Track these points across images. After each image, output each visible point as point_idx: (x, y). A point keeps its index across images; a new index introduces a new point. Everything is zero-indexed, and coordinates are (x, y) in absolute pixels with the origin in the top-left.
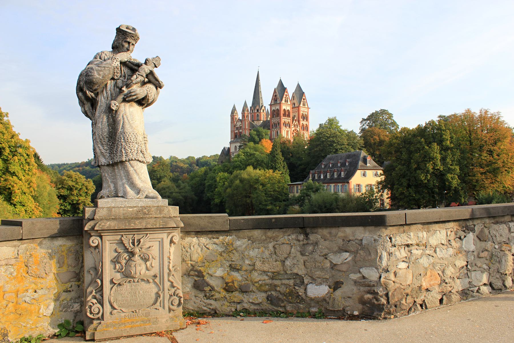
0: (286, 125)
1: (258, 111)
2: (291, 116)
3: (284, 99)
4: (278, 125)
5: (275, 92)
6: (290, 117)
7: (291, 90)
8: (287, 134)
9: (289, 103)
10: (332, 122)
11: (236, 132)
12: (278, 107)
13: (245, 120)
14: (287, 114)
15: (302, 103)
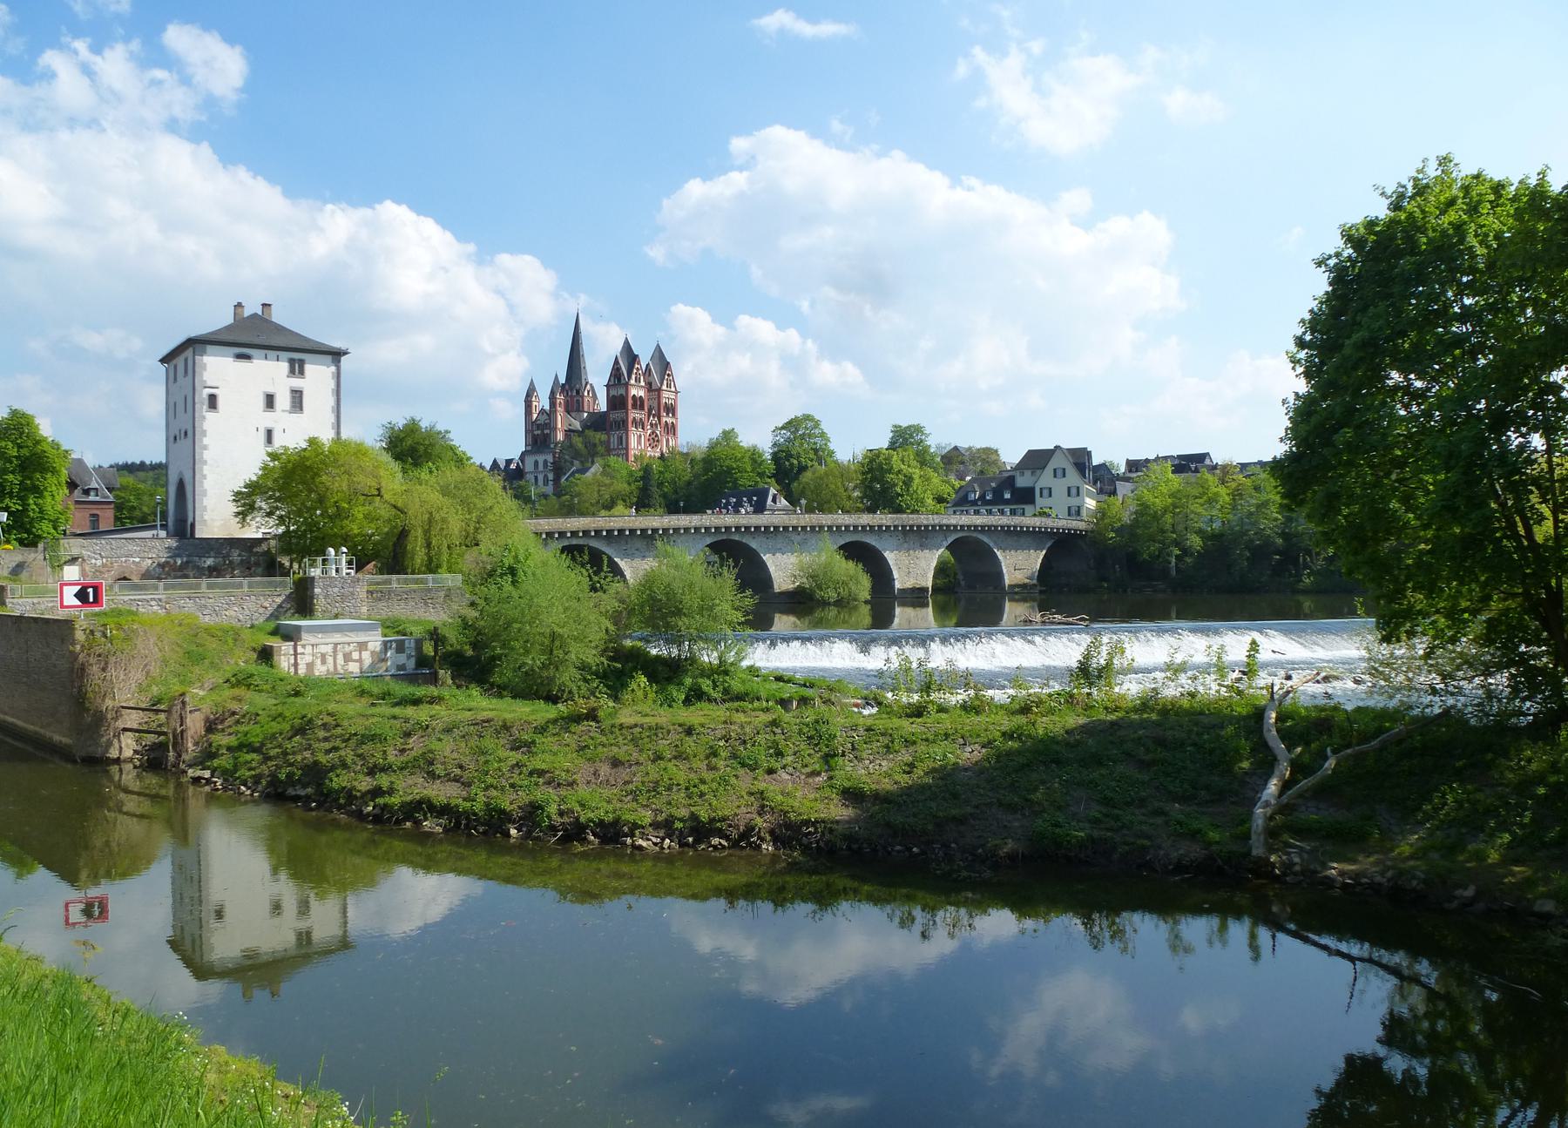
0: (636, 423)
1: (578, 392)
2: (646, 408)
3: (633, 376)
4: (622, 425)
5: (616, 362)
6: (643, 410)
7: (645, 359)
8: (639, 443)
9: (643, 384)
10: (728, 435)
11: (536, 433)
12: (622, 391)
13: (556, 411)
14: (638, 403)
15: (665, 382)
